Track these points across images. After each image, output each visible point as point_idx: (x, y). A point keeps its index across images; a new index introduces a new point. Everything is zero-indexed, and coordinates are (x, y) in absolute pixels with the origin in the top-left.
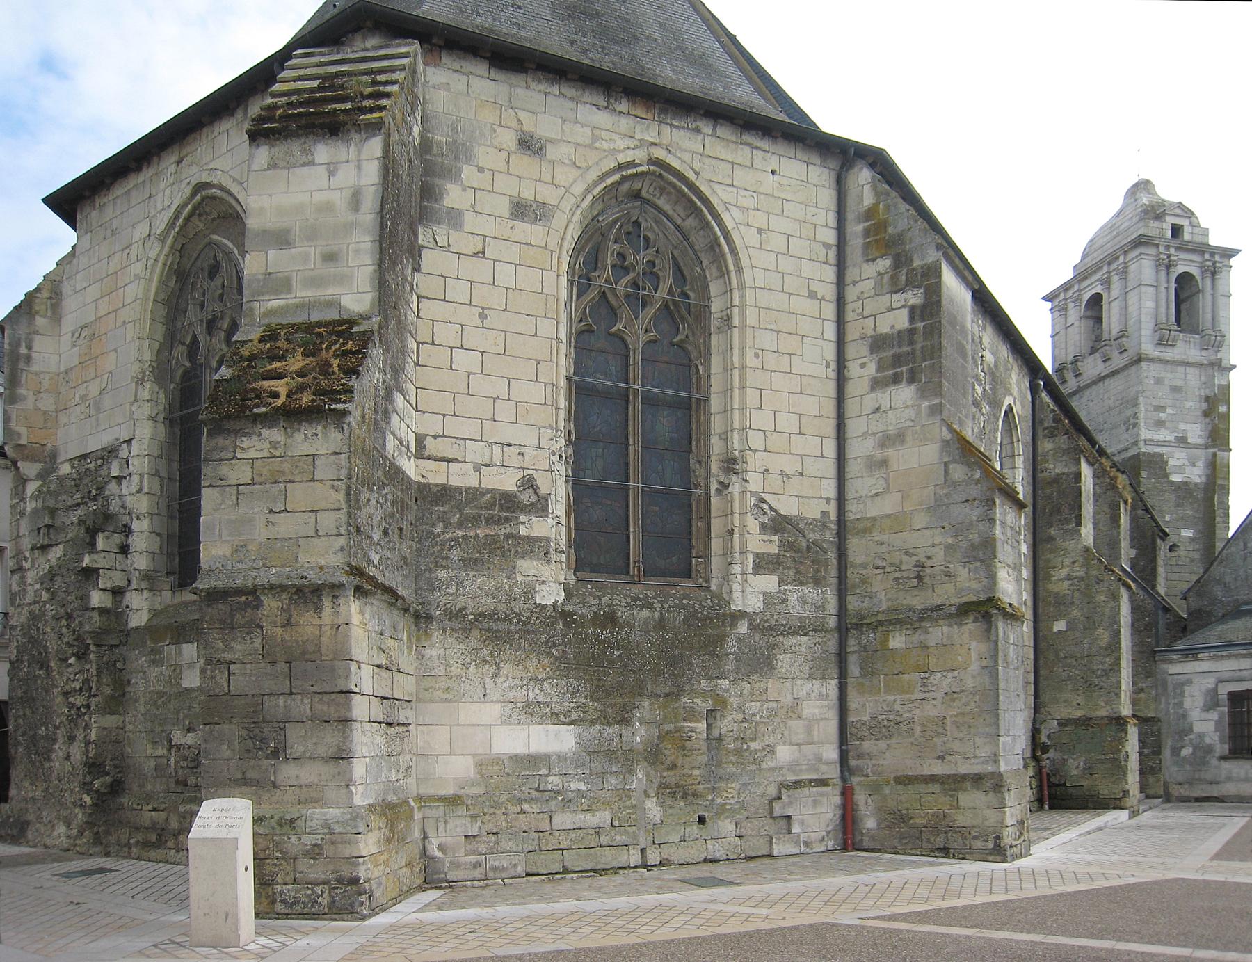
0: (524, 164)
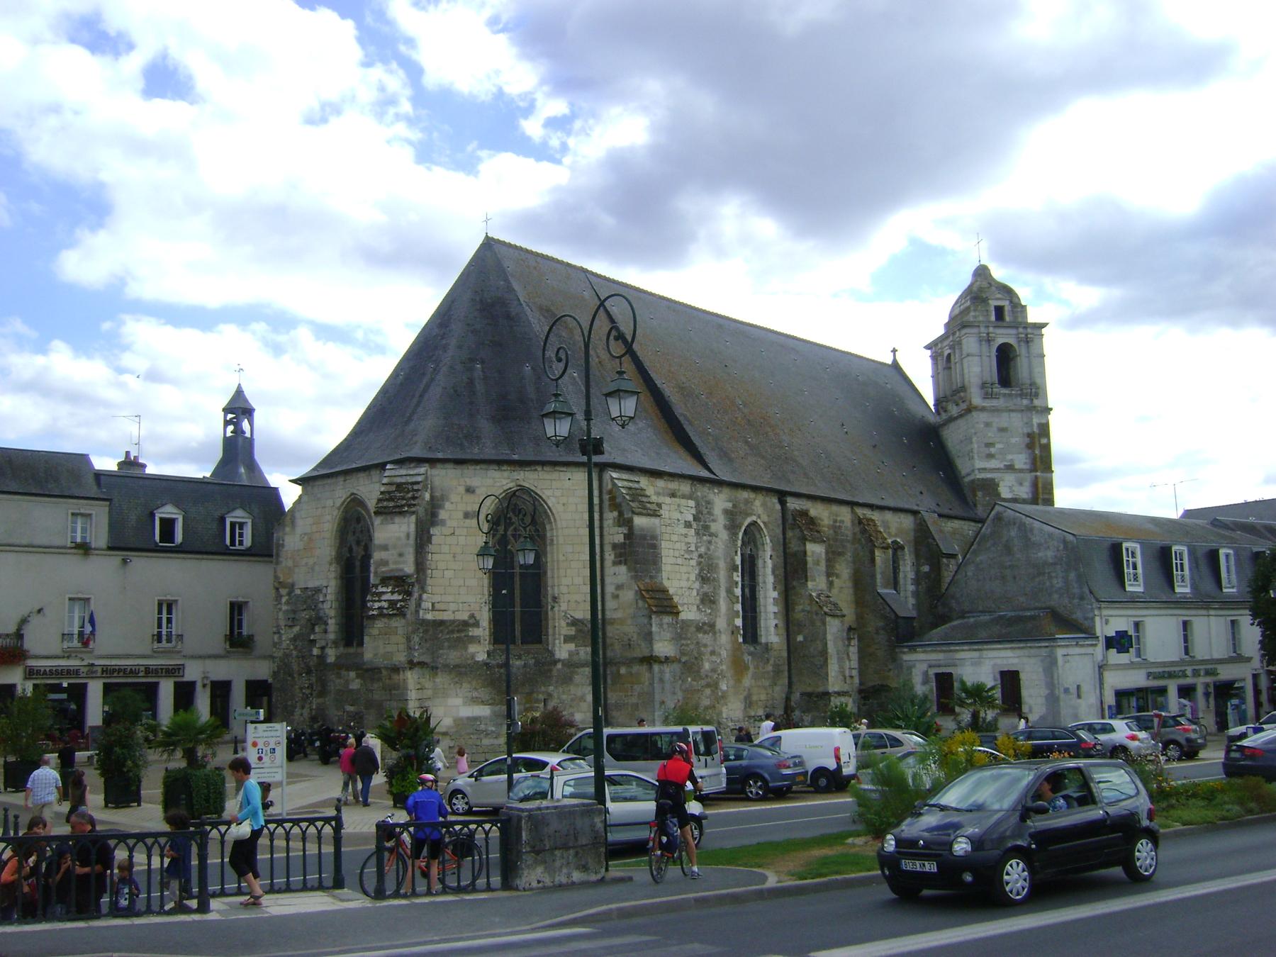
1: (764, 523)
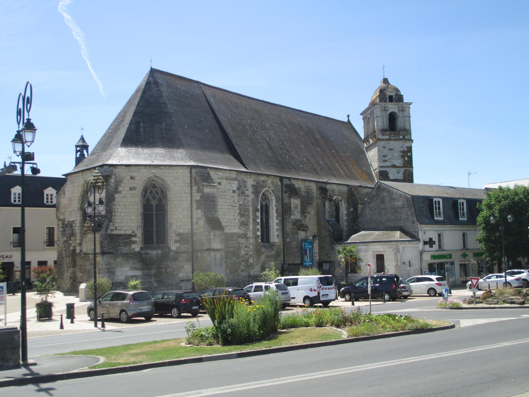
0: (132, 181)
1: (272, 191)
